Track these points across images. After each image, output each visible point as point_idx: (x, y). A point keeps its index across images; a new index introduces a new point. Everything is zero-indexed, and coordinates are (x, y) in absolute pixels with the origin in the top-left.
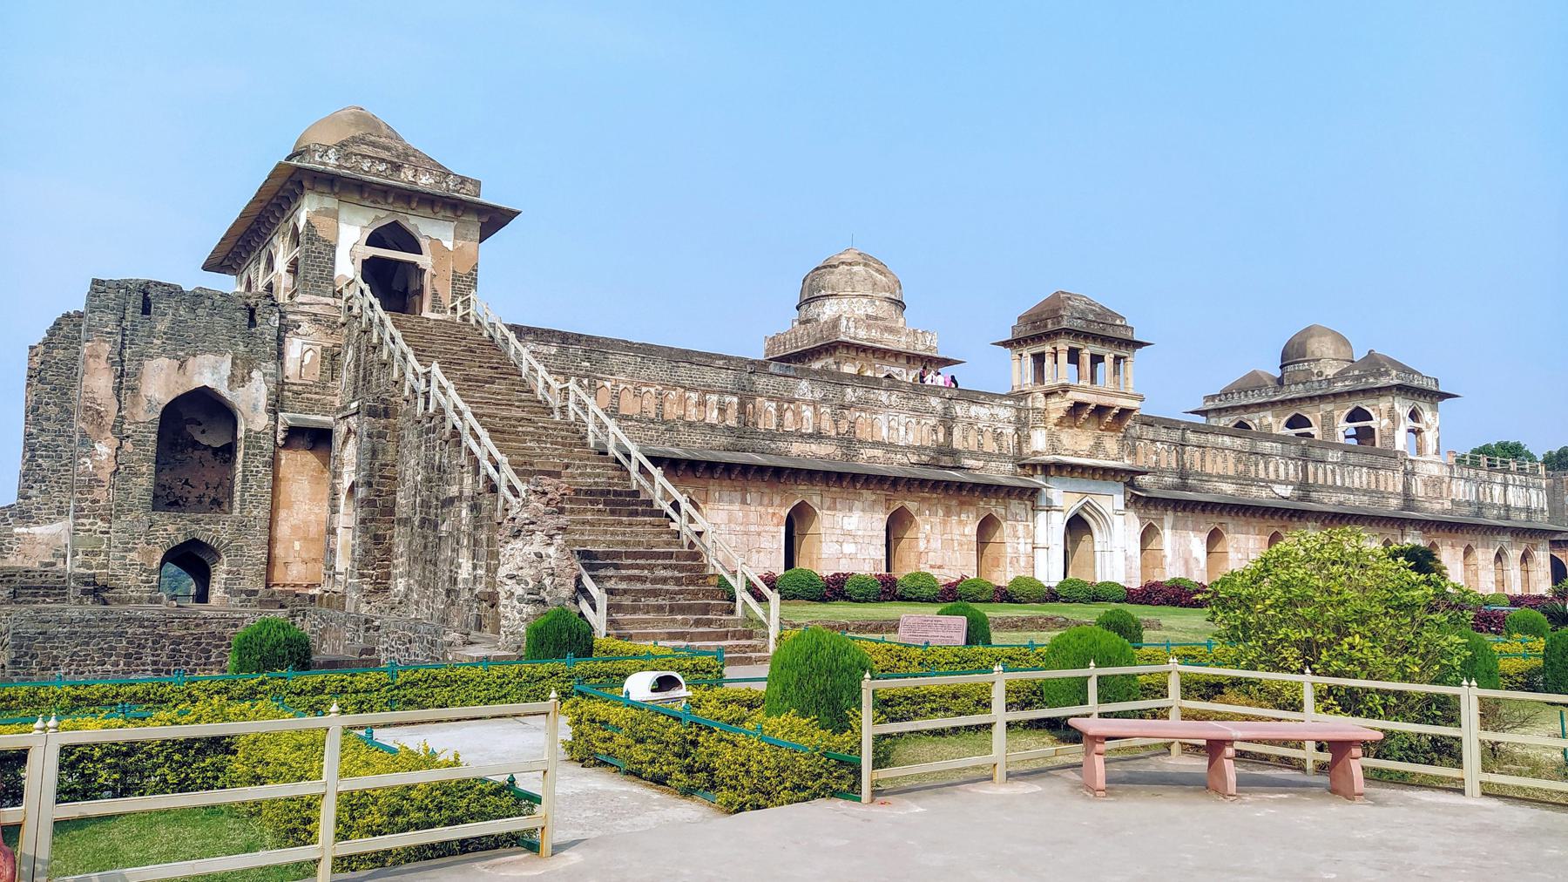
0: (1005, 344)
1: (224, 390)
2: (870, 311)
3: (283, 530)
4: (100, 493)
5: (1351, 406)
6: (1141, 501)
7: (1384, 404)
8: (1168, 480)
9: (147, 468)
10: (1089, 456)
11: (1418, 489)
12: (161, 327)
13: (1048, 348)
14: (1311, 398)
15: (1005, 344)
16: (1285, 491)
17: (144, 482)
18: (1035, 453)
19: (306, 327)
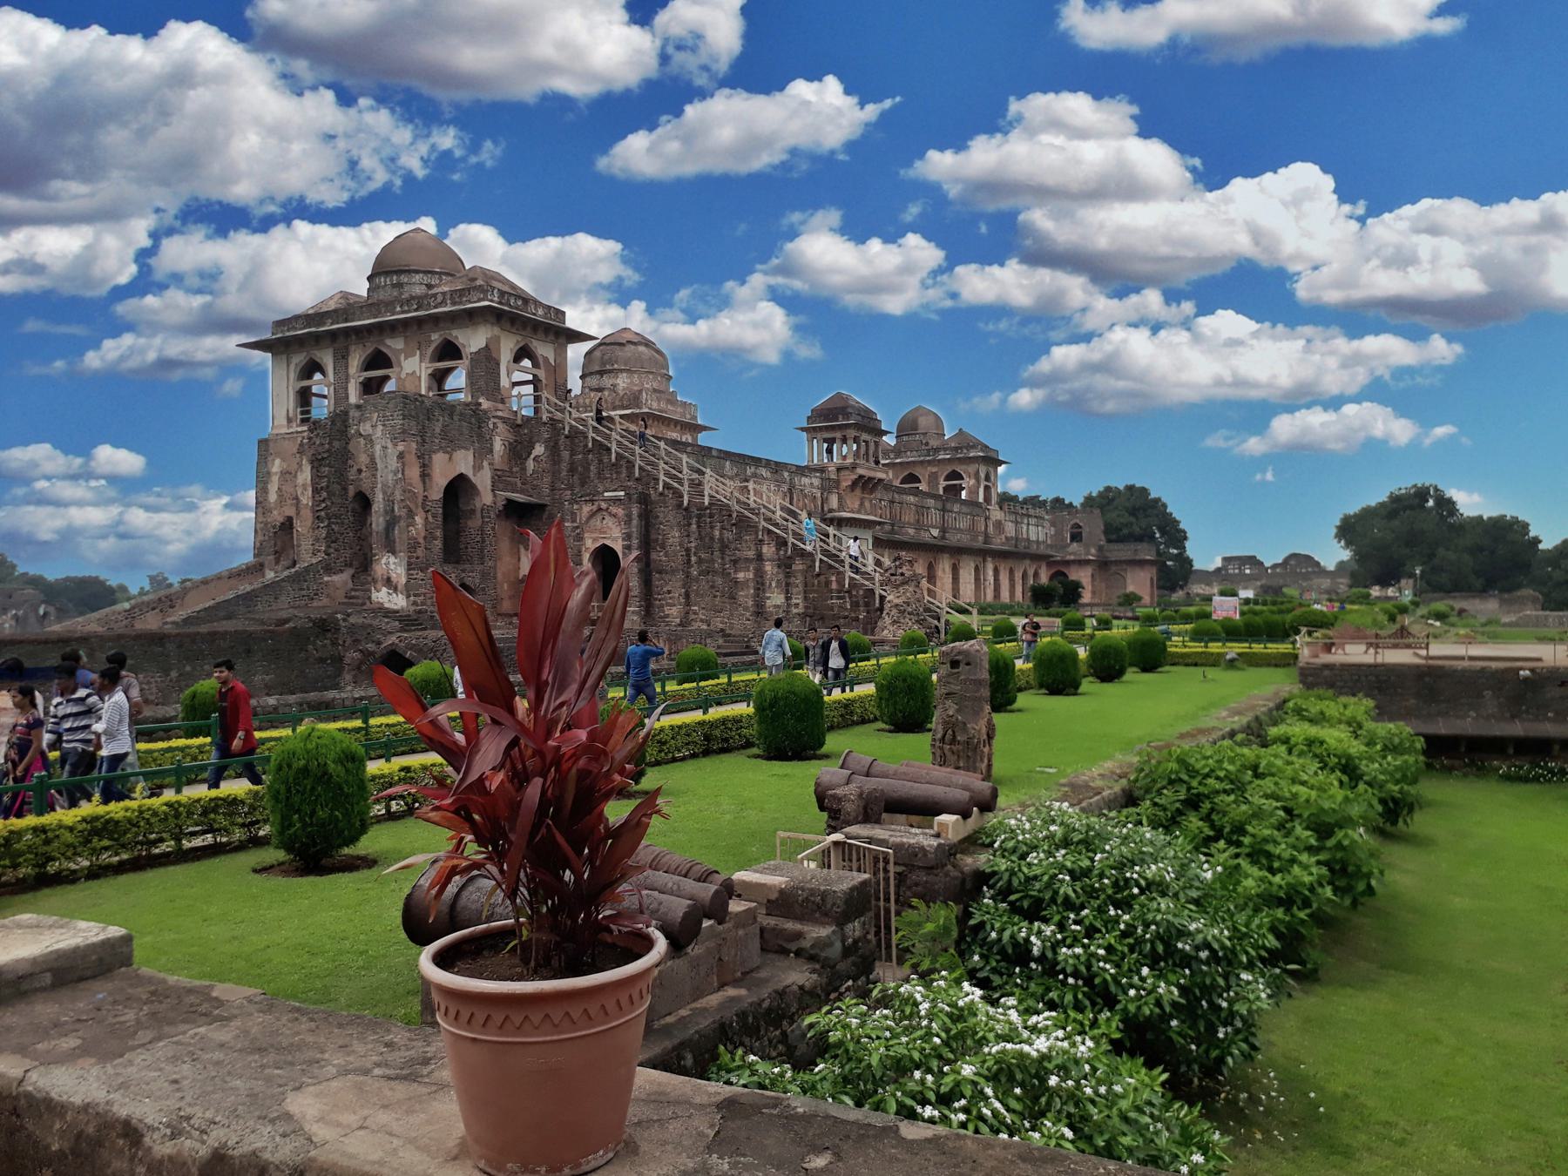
0: (802, 429)
1: (470, 474)
2: (655, 385)
3: (499, 576)
4: (420, 552)
5: (949, 469)
6: (879, 543)
7: (972, 468)
8: (888, 528)
9: (439, 533)
10: (859, 512)
11: (991, 529)
12: (438, 430)
13: (838, 435)
14: (922, 462)
15: (802, 429)
16: (935, 532)
17: (438, 544)
18: (831, 511)
19: (500, 425)
